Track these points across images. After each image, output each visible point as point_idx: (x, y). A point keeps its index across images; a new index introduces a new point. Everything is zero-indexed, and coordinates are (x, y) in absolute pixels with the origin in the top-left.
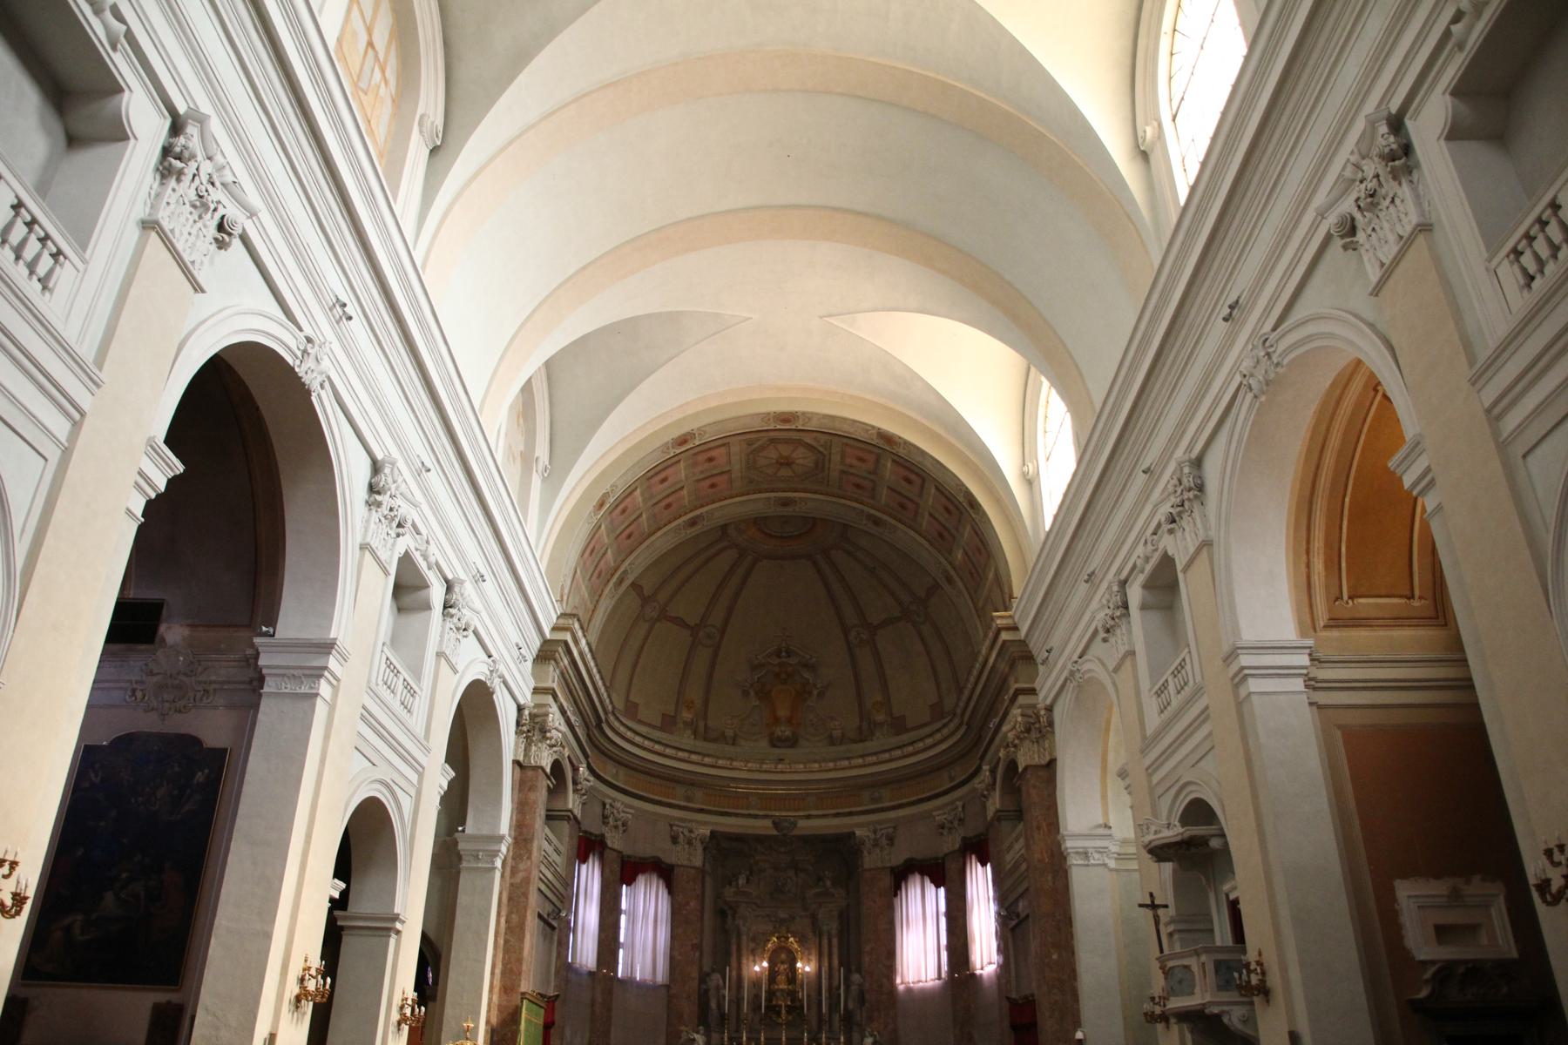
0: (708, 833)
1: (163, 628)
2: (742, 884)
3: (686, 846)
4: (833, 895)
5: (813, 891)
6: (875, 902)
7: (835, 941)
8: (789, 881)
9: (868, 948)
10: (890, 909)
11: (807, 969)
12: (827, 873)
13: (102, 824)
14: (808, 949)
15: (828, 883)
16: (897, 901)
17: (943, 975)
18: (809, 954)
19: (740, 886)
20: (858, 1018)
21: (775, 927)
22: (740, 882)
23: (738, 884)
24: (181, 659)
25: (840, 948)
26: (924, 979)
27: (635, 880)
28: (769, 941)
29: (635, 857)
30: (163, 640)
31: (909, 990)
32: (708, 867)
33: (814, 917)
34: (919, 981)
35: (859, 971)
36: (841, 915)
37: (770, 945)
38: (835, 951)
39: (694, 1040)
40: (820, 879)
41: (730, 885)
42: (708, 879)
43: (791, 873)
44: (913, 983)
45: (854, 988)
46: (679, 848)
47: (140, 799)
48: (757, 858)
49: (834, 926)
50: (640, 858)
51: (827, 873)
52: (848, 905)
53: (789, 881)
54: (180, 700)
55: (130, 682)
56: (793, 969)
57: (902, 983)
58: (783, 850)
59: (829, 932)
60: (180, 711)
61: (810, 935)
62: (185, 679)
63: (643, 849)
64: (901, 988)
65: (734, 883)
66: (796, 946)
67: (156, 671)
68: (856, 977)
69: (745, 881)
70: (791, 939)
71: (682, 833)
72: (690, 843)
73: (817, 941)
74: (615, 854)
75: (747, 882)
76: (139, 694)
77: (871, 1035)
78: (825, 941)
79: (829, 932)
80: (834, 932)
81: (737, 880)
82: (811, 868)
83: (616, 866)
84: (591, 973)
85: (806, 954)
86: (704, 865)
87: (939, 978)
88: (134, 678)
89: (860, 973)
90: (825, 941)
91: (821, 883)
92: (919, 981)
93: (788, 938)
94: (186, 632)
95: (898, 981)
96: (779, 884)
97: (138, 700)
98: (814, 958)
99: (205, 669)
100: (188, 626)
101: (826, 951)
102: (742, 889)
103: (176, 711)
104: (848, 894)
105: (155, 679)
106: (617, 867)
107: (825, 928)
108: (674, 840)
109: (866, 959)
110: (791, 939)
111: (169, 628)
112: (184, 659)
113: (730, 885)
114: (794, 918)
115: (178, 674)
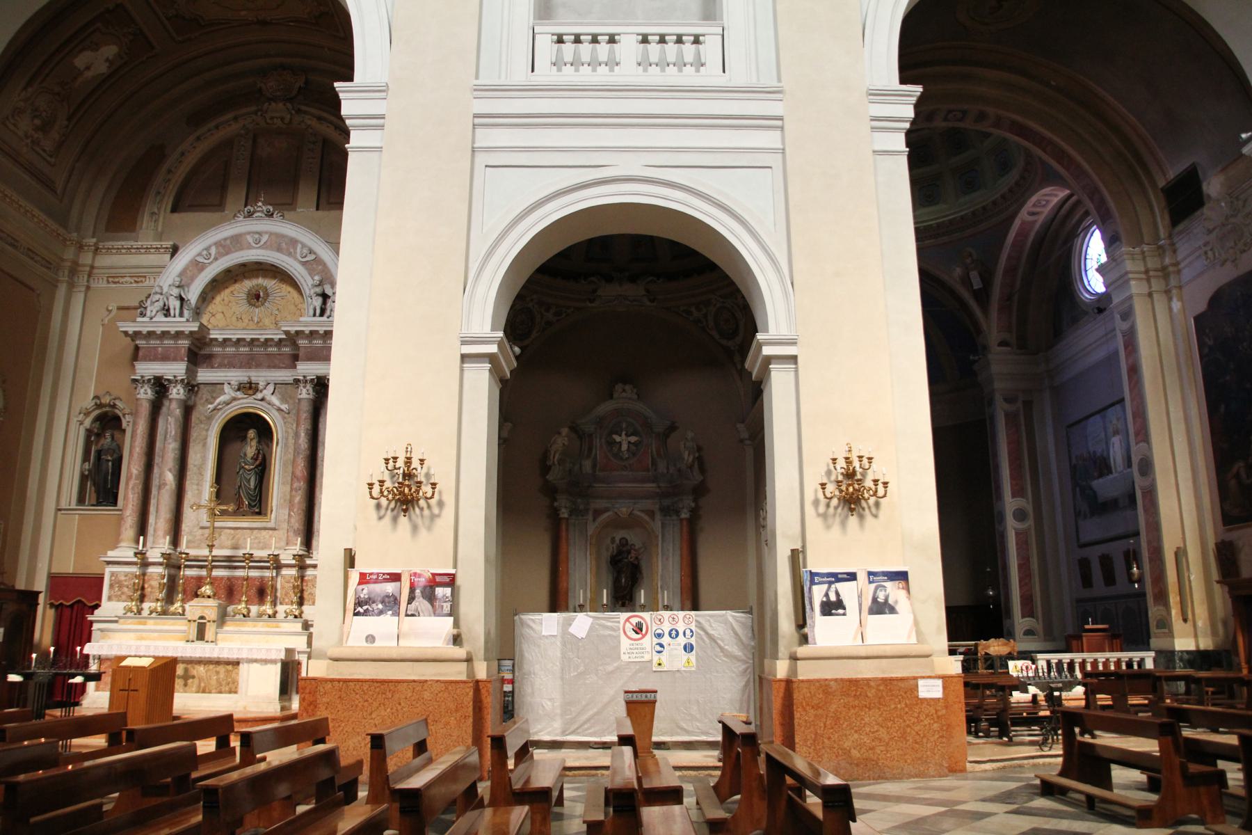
1: (1204, 187)
13: (1228, 378)
24: (1223, 204)
30: (1209, 196)
47: (1245, 344)
54: (1239, 240)
55: (1200, 248)
60: (1244, 251)
62: (1232, 220)
67: (1211, 227)
76: (1210, 254)
88: (1201, 243)
94: (1221, 178)
97: (1212, 259)
99: (1245, 201)
100: (1223, 170)
103: (1241, 253)
105: (1214, 233)
111: (1209, 184)
112: (1226, 203)
115: (1227, 219)
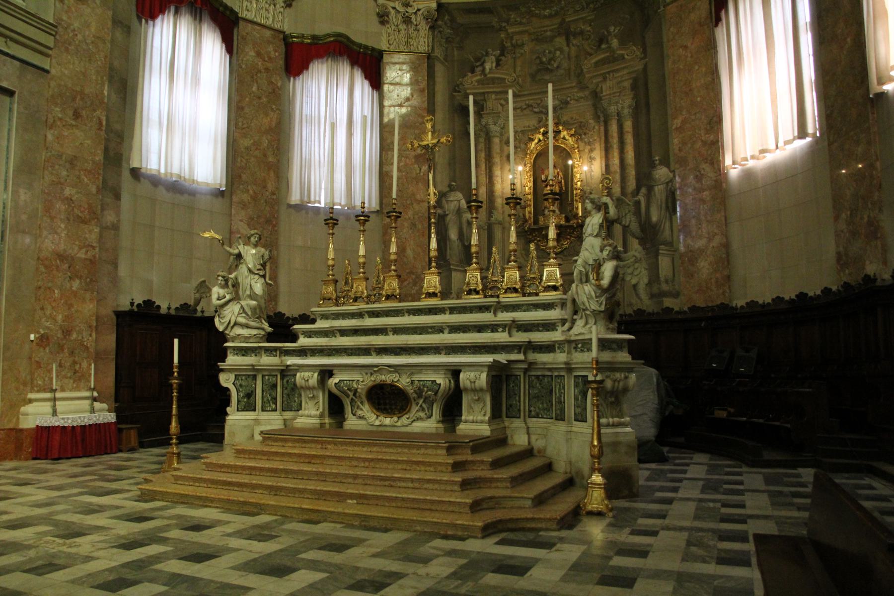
0: (434, 5)
2: (490, 69)
3: (403, 27)
4: (623, 57)
5: (594, 61)
6: (686, 47)
7: (628, 125)
8: (558, 53)
9: (677, 122)
10: (711, 47)
11: (585, 168)
12: (612, 29)
14: (589, 143)
15: (615, 43)
16: (720, 33)
17: (810, 130)
18: (591, 151)
19: (487, 70)
20: (667, 233)
21: (540, 122)
22: (488, 66)
23: (484, 70)
25: (636, 136)
26: (772, 146)
27: (307, 68)
28: (533, 140)
29: (303, 36)
31: (748, 175)
32: (438, 53)
33: (596, 96)
34: (763, 151)
35: (666, 162)
36: (634, 87)
37: (533, 145)
38: (629, 139)
39: (239, 256)
40: (601, 41)
41: (473, 71)
42: (440, 70)
43: (560, 41)
44: (753, 157)
45: (659, 191)
46: (390, 28)
48: (511, 30)
49: (626, 103)
50: (314, 37)
51: (612, 29)
52: (646, 65)
53: (558, 53)
56: (568, 173)
57: (734, 163)
58: (547, 12)
59: (618, 114)
61: (591, 121)
63: (323, 28)
64: (734, 173)
65: (479, 69)
66: (571, 141)
68: (661, 173)
69: (494, 65)
70: (564, 133)
71: (394, 8)
72: (407, 20)
73: (602, 128)
74: (268, 33)
75: (498, 65)
77: (598, 208)
78: (614, 128)
79: (618, 114)
80: (626, 111)
81: (482, 65)
82: (589, 28)
83: (270, 49)
84: (219, 194)
85: (587, 151)
86: (433, 49)
87: (802, 133)
89: (668, 165)
90: (614, 128)
91: (603, 46)
92: (763, 151)
93: (560, 131)
95: (728, 161)
96: (544, 60)
98: (598, 154)
101: (615, 141)
102: (489, 76)
104: (645, 51)
106: (276, 53)
107: (613, 109)
108: (383, 18)
109: (675, 141)
110: (564, 133)
113: (473, 71)
114: (567, 103)
